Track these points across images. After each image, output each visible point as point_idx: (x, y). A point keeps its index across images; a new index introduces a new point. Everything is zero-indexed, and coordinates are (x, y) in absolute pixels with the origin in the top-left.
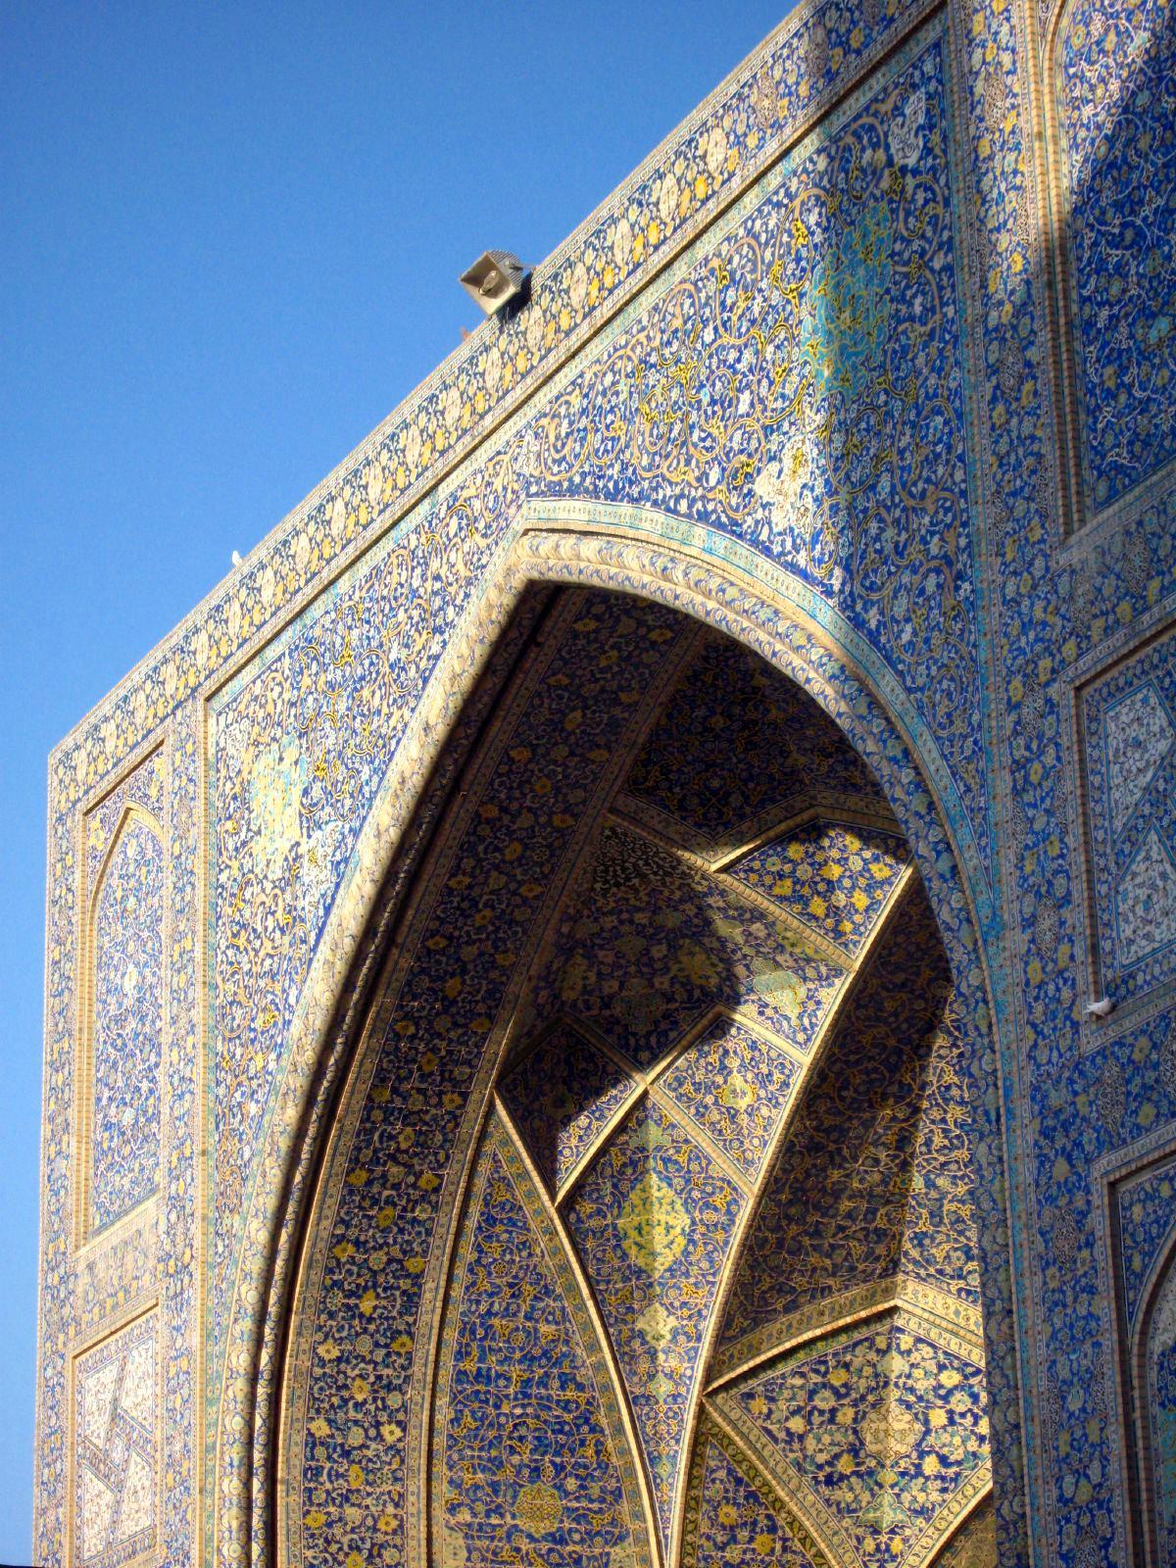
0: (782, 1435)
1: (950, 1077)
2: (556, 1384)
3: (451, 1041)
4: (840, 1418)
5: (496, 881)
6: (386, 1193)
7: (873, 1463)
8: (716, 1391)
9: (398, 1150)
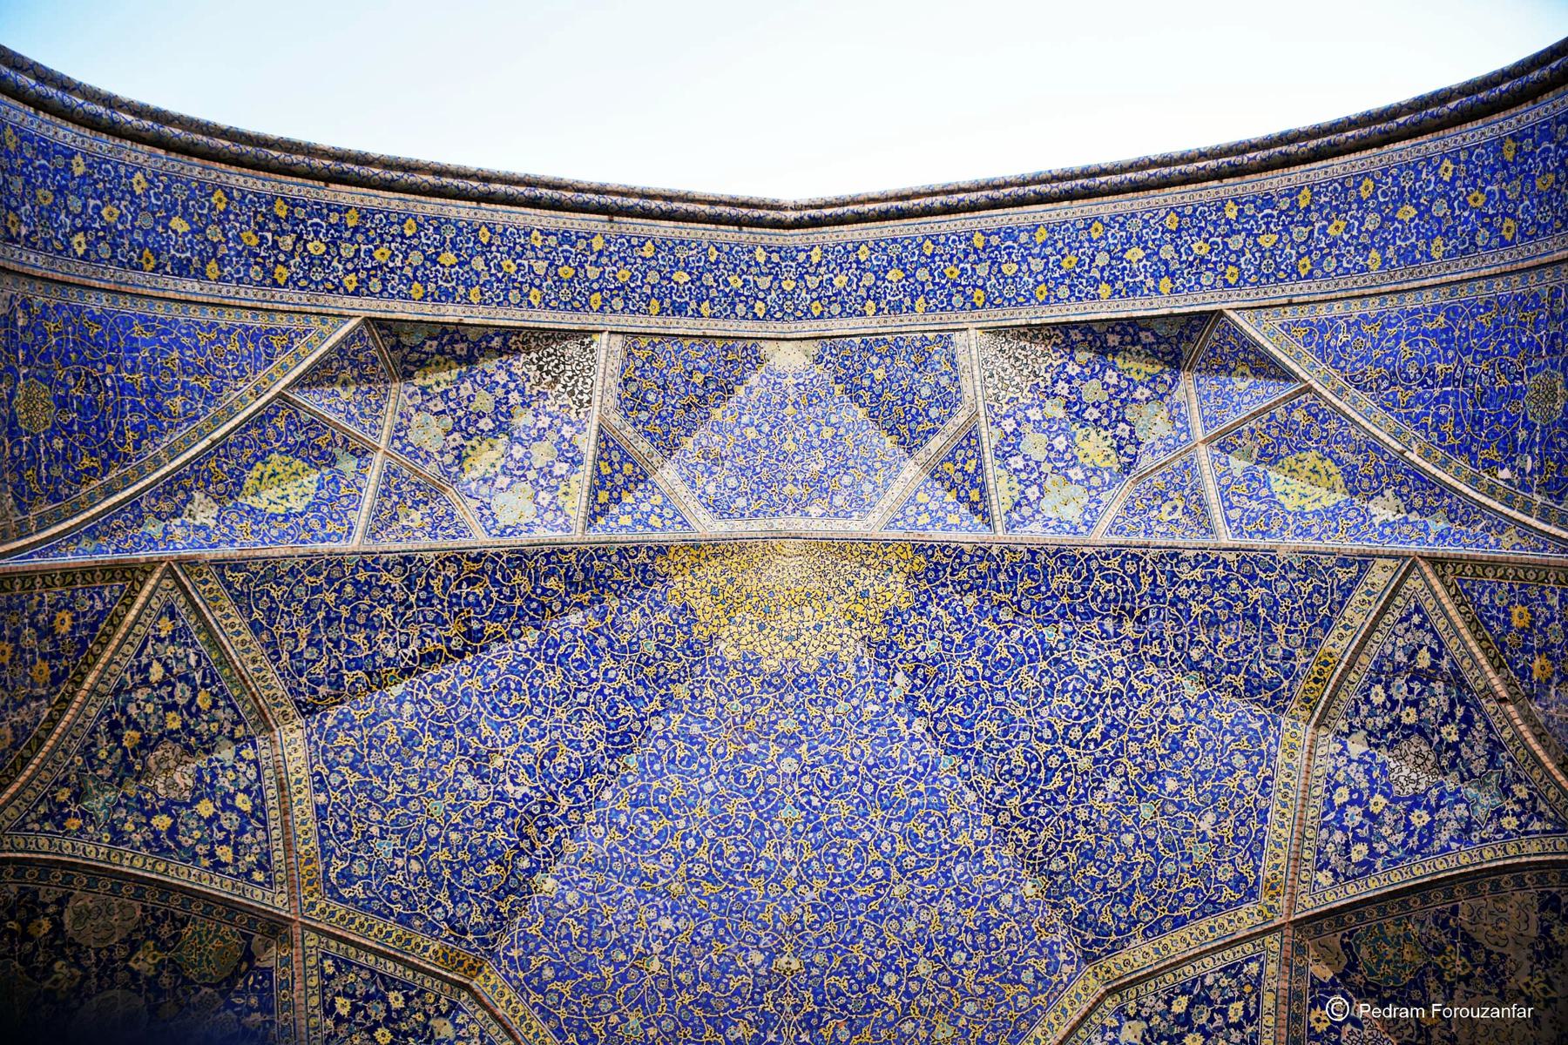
0: (145, 660)
1: (502, 665)
2: (136, 420)
4: (171, 715)
5: (540, 267)
6: (269, 235)
7: (138, 768)
9: (306, 242)
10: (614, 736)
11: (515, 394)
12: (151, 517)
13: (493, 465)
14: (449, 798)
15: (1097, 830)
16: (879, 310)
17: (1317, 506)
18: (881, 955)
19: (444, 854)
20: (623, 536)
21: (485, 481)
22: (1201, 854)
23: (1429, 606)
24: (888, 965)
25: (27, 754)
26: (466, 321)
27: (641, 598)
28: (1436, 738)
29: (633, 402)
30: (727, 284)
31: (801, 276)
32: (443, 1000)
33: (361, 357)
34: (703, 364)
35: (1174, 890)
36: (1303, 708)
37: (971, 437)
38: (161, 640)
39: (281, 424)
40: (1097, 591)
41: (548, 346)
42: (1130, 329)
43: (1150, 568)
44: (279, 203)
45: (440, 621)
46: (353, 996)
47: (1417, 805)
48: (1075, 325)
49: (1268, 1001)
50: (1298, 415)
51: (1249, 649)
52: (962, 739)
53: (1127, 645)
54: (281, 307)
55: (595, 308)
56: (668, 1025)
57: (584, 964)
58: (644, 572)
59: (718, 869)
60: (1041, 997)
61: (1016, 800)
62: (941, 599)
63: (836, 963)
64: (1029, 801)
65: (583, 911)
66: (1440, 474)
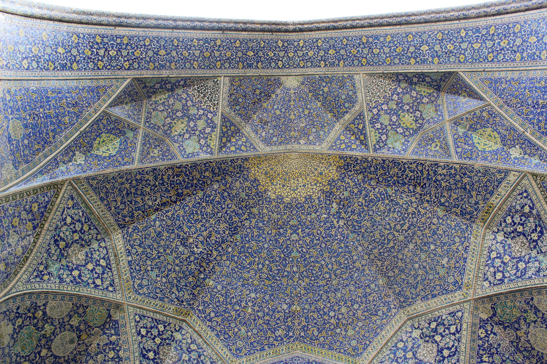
0: (64, 216)
1: (190, 205)
2: (52, 128)
3: (145, 58)
4: (75, 234)
5: (197, 53)
7: (66, 254)
8: (72, 185)
9: (109, 51)
10: (231, 228)
11: (190, 102)
12: (61, 163)
13: (183, 130)
14: (174, 255)
15: (405, 262)
16: (326, 65)
17: (490, 149)
18: (329, 305)
19: (174, 275)
20: (232, 155)
21: (180, 136)
22: (442, 272)
23: (530, 190)
24: (331, 309)
25: (28, 255)
26: (170, 76)
27: (239, 177)
28: (529, 238)
29: (233, 103)
30: (268, 55)
31: (296, 51)
32: (177, 326)
33: (132, 93)
34: (259, 86)
35: (432, 285)
36: (481, 222)
37: (361, 115)
38: (69, 208)
39: (105, 122)
40: (407, 176)
41: (201, 83)
42: (422, 77)
43: (427, 168)
44: (98, 37)
45: (167, 191)
46: (146, 328)
47: (521, 261)
48: (401, 74)
49: (464, 326)
50: (485, 114)
51: (462, 200)
52: (357, 228)
53: (417, 196)
54: (101, 77)
55: (218, 67)
56: (255, 331)
57: (225, 311)
58: (240, 167)
59: (270, 275)
60: (385, 320)
61: (376, 251)
62: (350, 176)
63: (313, 308)
64: (381, 251)
65: (223, 292)
66: (537, 142)
